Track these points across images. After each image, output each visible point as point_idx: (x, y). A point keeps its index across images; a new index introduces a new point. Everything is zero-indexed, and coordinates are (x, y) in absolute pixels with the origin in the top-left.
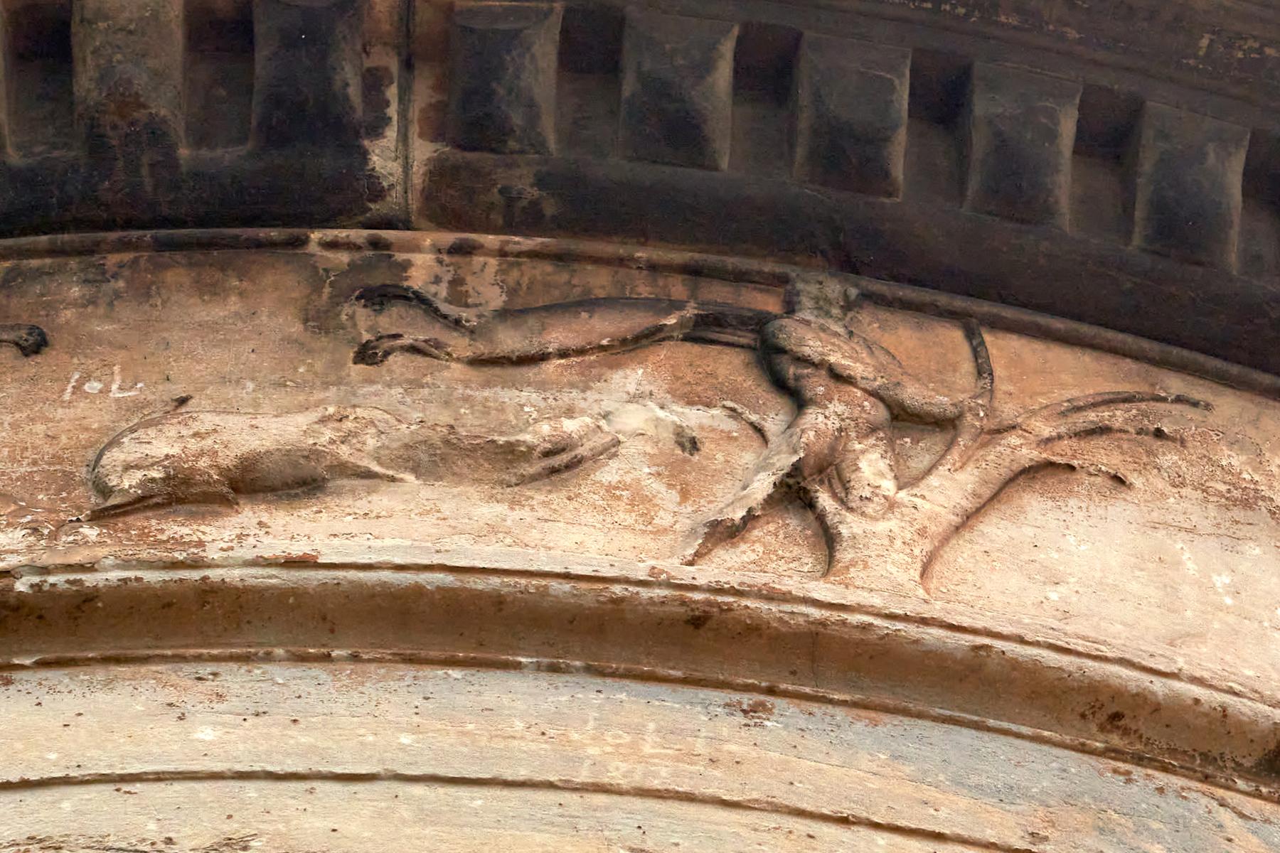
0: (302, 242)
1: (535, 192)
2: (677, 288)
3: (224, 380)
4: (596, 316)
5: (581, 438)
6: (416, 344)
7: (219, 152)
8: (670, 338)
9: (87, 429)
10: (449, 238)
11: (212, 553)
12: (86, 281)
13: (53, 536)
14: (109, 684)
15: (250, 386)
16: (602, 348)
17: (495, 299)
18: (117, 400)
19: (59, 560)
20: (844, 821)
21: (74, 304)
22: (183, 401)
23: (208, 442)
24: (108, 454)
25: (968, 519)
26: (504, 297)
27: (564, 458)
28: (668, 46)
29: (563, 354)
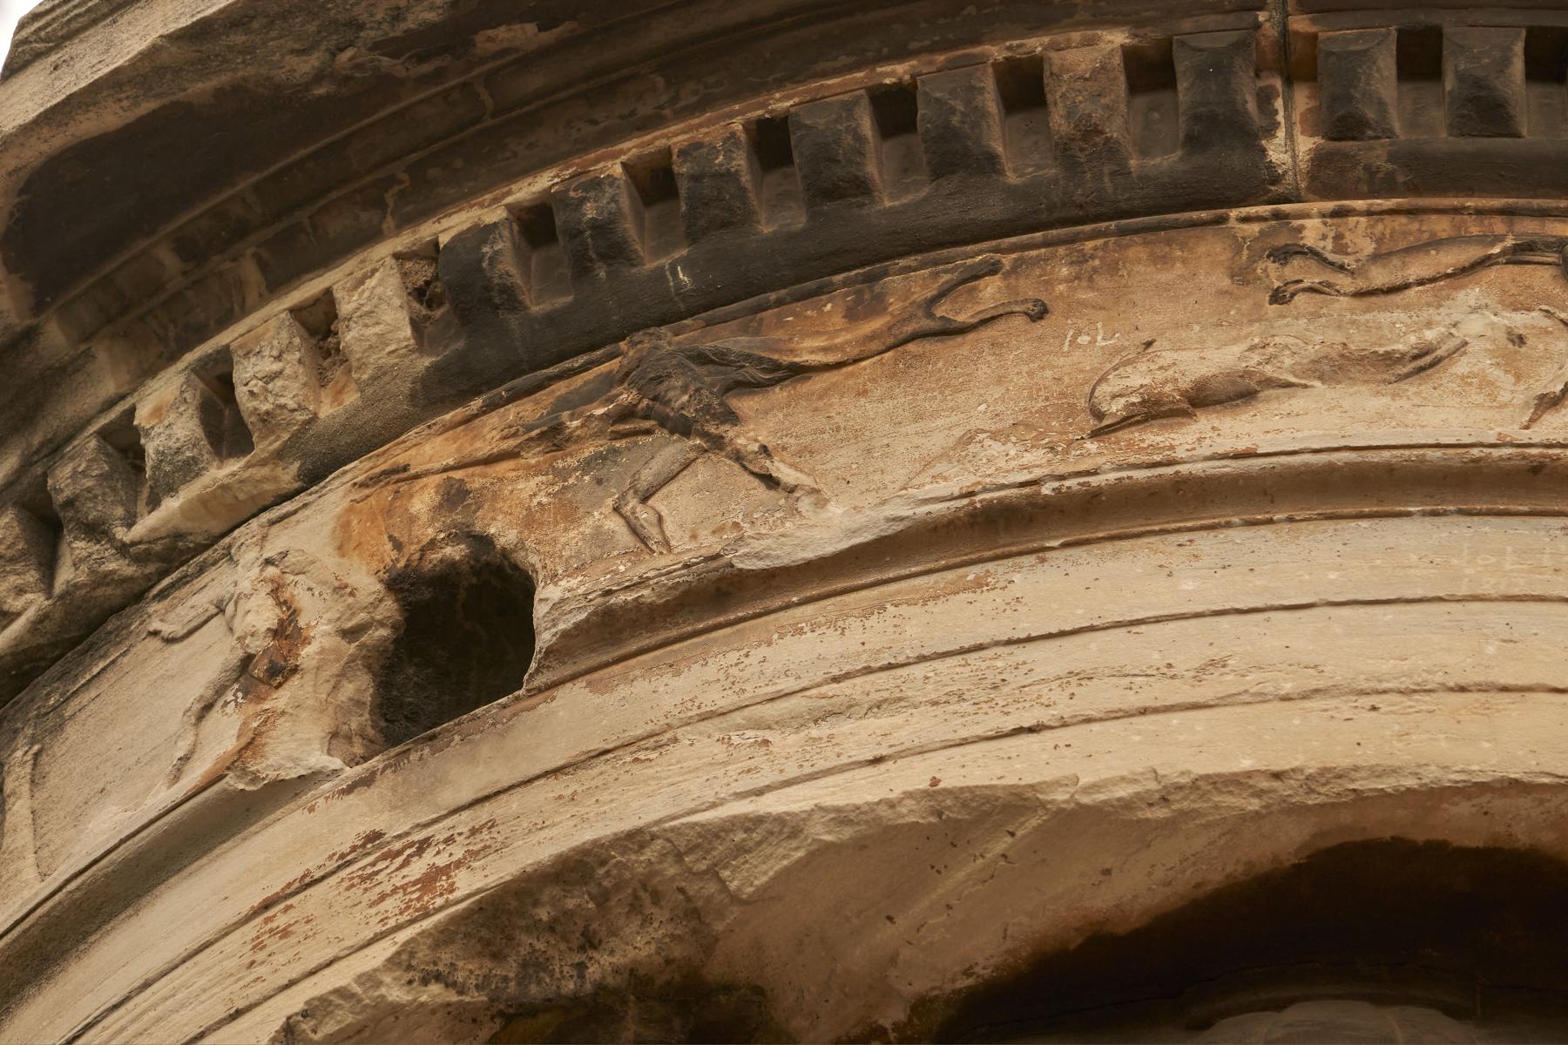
0: (1223, 220)
1: (1390, 167)
2: (1499, 225)
3: (1177, 326)
4: (1441, 253)
5: (1438, 343)
6: (1313, 286)
7: (1158, 160)
8: (1497, 263)
9: (1082, 371)
10: (1330, 205)
11: (1180, 453)
12: (1072, 263)
13: (1066, 452)
14: (1115, 554)
15: (1197, 328)
16: (1448, 276)
17: (1369, 247)
18: (1102, 348)
19: (1071, 469)
21: (1067, 280)
22: (1149, 344)
23: (1170, 372)
24: (1099, 388)
26: (1374, 245)
27: (1428, 359)
28: (1475, 51)
29: (1421, 282)
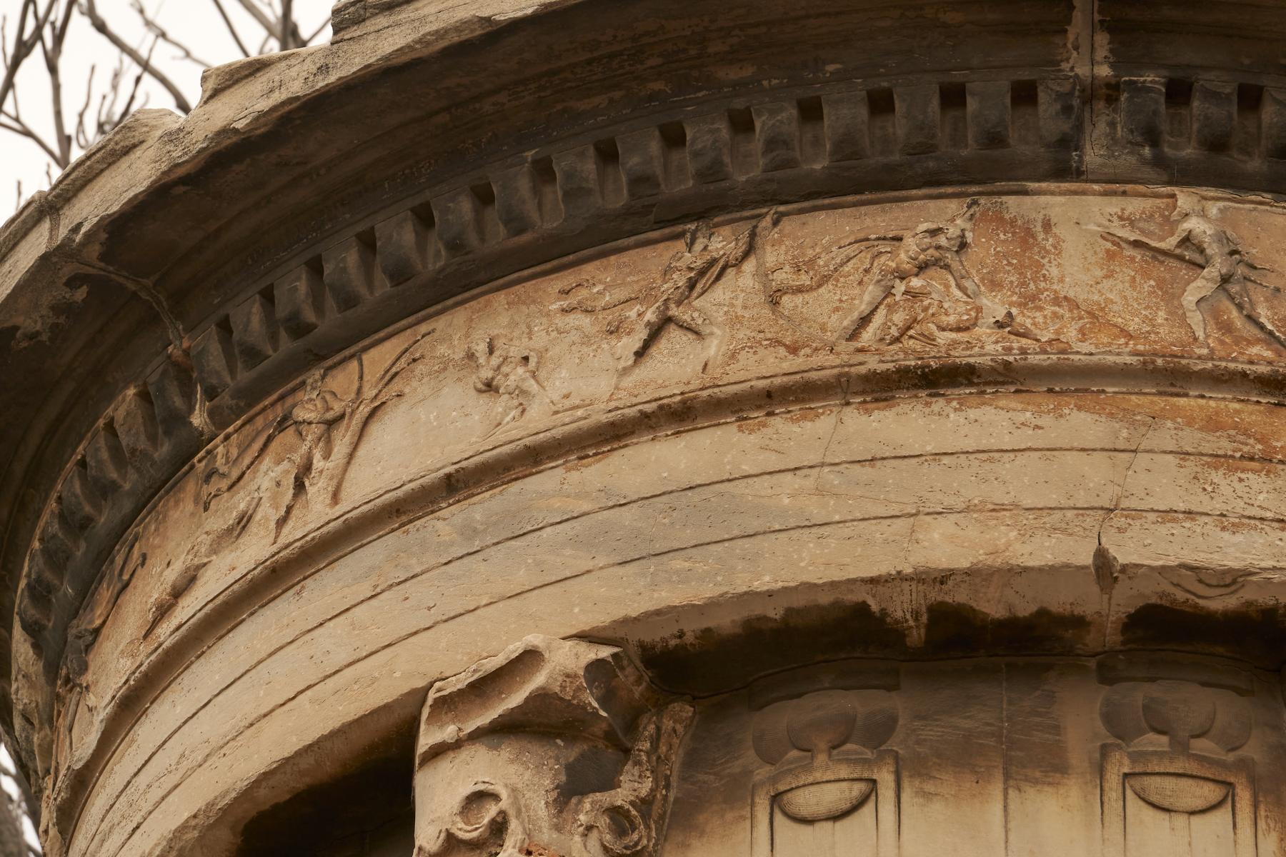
16: (257, 457)
20: (321, 624)
25: (351, 456)
27: (245, 519)
29: (248, 468)
